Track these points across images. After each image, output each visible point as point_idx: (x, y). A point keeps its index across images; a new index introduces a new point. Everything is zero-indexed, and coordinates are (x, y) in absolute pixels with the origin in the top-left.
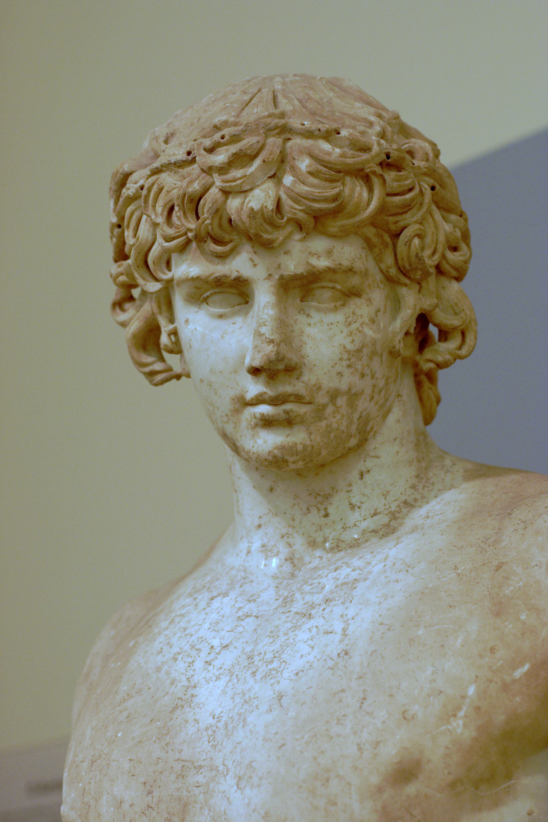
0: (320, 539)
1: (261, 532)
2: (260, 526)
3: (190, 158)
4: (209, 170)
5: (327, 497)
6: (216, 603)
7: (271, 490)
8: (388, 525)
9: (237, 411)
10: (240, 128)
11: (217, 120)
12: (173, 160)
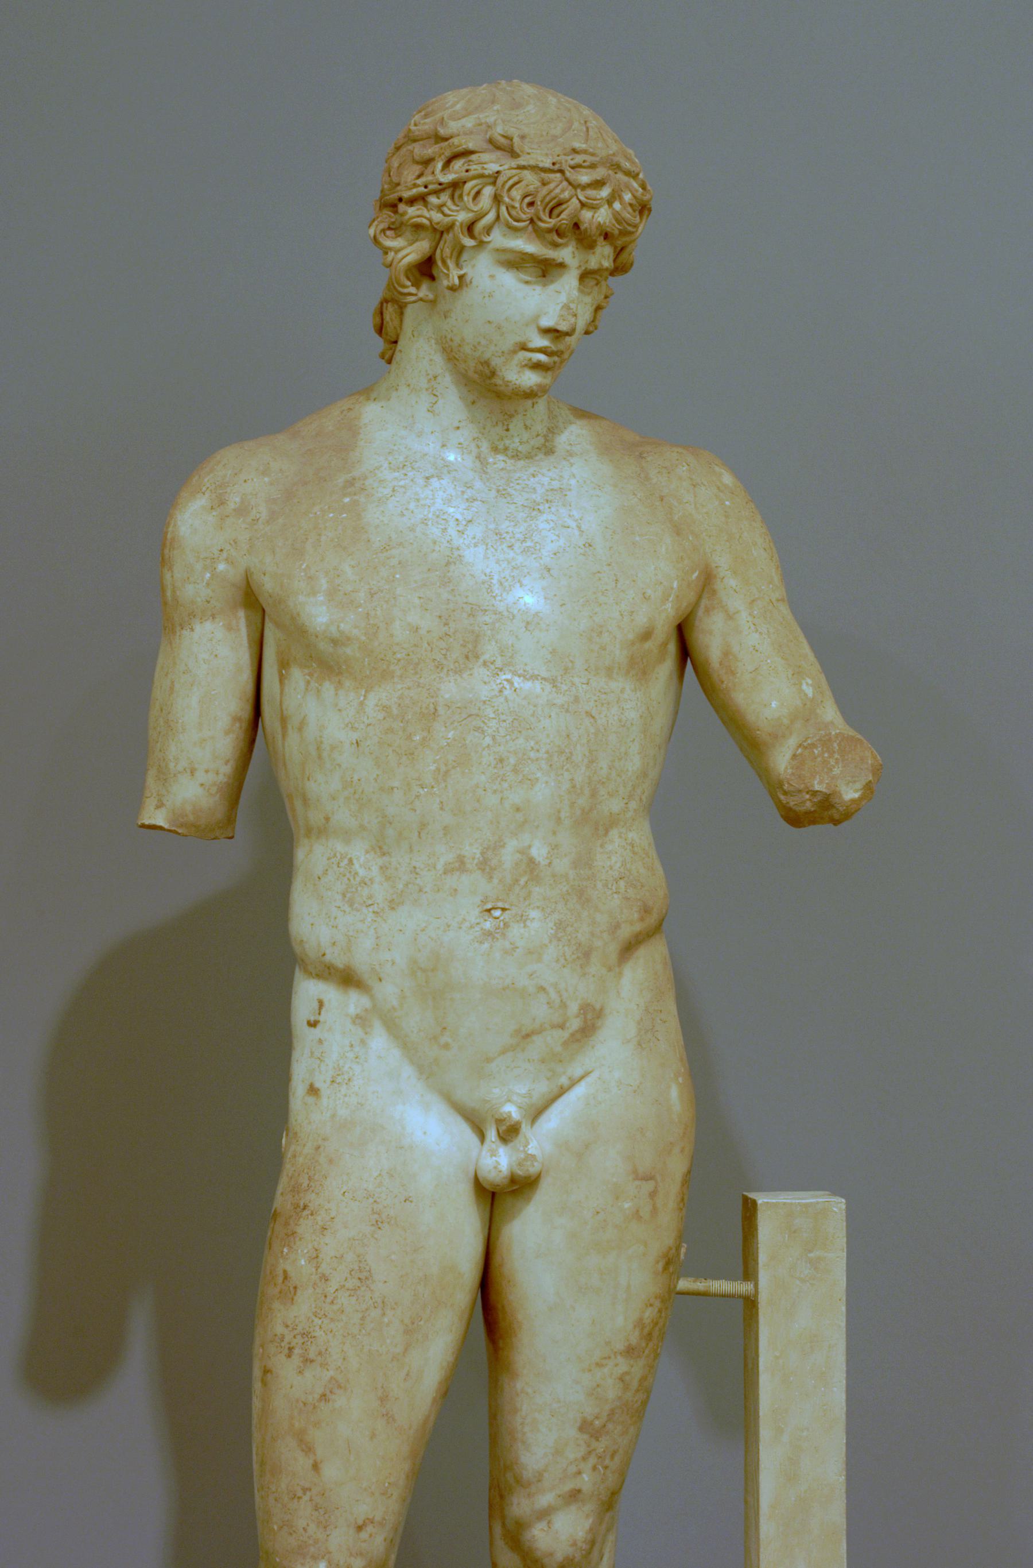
0: (501, 447)
1: (458, 432)
2: (458, 428)
3: (556, 167)
4: (575, 186)
5: (511, 416)
6: (435, 483)
7: (473, 403)
8: (544, 445)
9: (515, 352)
10: (598, 159)
11: (577, 145)
12: (541, 165)
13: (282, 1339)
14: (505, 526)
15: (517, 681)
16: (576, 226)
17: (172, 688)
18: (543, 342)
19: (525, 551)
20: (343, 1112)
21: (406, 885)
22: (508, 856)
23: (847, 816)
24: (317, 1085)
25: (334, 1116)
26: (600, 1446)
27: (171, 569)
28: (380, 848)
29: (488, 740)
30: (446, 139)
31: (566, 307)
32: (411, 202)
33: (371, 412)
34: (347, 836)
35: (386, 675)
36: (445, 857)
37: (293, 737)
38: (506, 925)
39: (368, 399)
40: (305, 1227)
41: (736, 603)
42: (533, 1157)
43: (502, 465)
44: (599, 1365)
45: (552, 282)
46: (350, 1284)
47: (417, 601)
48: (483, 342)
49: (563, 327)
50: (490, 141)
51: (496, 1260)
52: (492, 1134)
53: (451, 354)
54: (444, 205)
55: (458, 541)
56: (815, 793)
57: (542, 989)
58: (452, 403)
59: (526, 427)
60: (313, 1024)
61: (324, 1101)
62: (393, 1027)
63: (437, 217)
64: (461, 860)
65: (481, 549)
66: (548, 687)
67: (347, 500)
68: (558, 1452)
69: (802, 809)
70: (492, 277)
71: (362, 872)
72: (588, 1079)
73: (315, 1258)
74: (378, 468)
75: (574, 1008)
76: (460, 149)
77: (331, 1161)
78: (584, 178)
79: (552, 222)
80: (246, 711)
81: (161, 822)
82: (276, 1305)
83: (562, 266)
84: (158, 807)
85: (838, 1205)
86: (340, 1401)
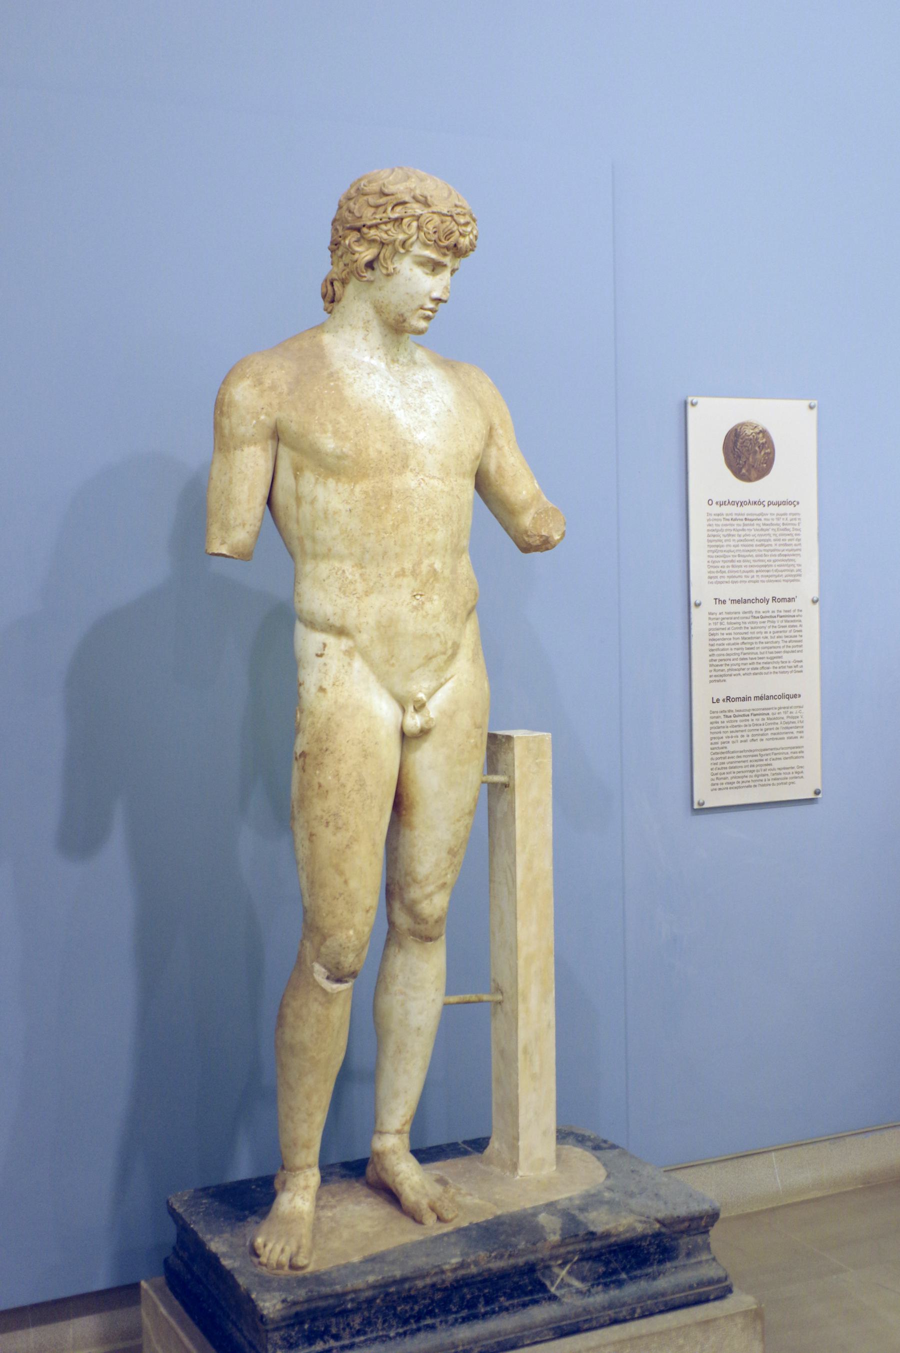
4: (458, 224)
9: (417, 310)
13: (322, 818)
14: (410, 400)
15: (426, 479)
16: (455, 245)
17: (231, 482)
18: (430, 305)
19: (423, 413)
20: (341, 700)
21: (375, 583)
22: (424, 568)
23: (554, 547)
24: (324, 687)
25: (336, 702)
26: (456, 861)
27: (229, 417)
28: (360, 565)
29: (416, 509)
30: (392, 195)
31: (446, 288)
32: (370, 227)
33: (327, 339)
34: (341, 558)
35: (365, 476)
36: (396, 569)
37: (306, 508)
38: (423, 603)
39: (323, 332)
40: (328, 760)
41: (502, 442)
42: (431, 719)
43: (397, 369)
44: (459, 821)
45: (437, 274)
46: (356, 787)
47: (379, 438)
48: (402, 304)
49: (444, 298)
50: (414, 198)
51: (405, 771)
52: (411, 709)
53: (379, 310)
54: (389, 230)
55: (391, 407)
56: (542, 536)
57: (438, 635)
58: (376, 335)
59: (406, 350)
60: (321, 655)
61: (329, 695)
62: (365, 655)
63: (385, 236)
64: (403, 570)
65: (402, 411)
66: (440, 482)
67: (332, 384)
68: (437, 865)
69: (535, 544)
70: (411, 270)
71: (350, 577)
72: (453, 679)
73: (337, 775)
74: (343, 368)
75: (450, 644)
76: (401, 201)
77: (338, 725)
78: (462, 220)
79: (446, 243)
80: (267, 495)
81: (224, 552)
82: (315, 800)
83: (445, 266)
84: (222, 544)
85: (548, 736)
86: (355, 847)
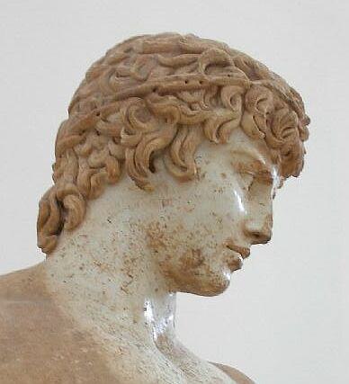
7: (156, 290)
32: (165, 93)
48: (203, 231)
53: (155, 241)
